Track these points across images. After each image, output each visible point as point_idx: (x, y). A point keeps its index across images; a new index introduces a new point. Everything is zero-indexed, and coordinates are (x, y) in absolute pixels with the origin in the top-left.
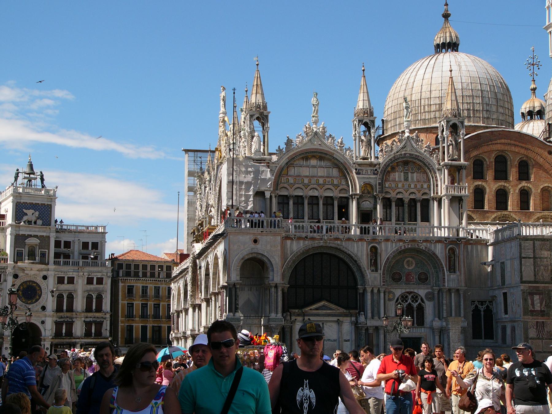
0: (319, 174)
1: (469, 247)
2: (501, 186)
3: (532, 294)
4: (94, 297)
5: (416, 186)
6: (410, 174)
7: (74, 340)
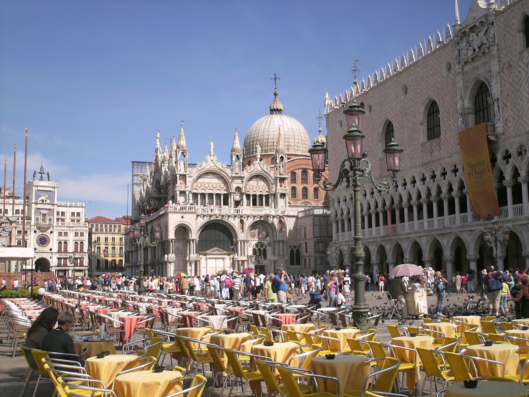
0: (213, 182)
3: (318, 243)
5: (262, 188)
7: (68, 268)
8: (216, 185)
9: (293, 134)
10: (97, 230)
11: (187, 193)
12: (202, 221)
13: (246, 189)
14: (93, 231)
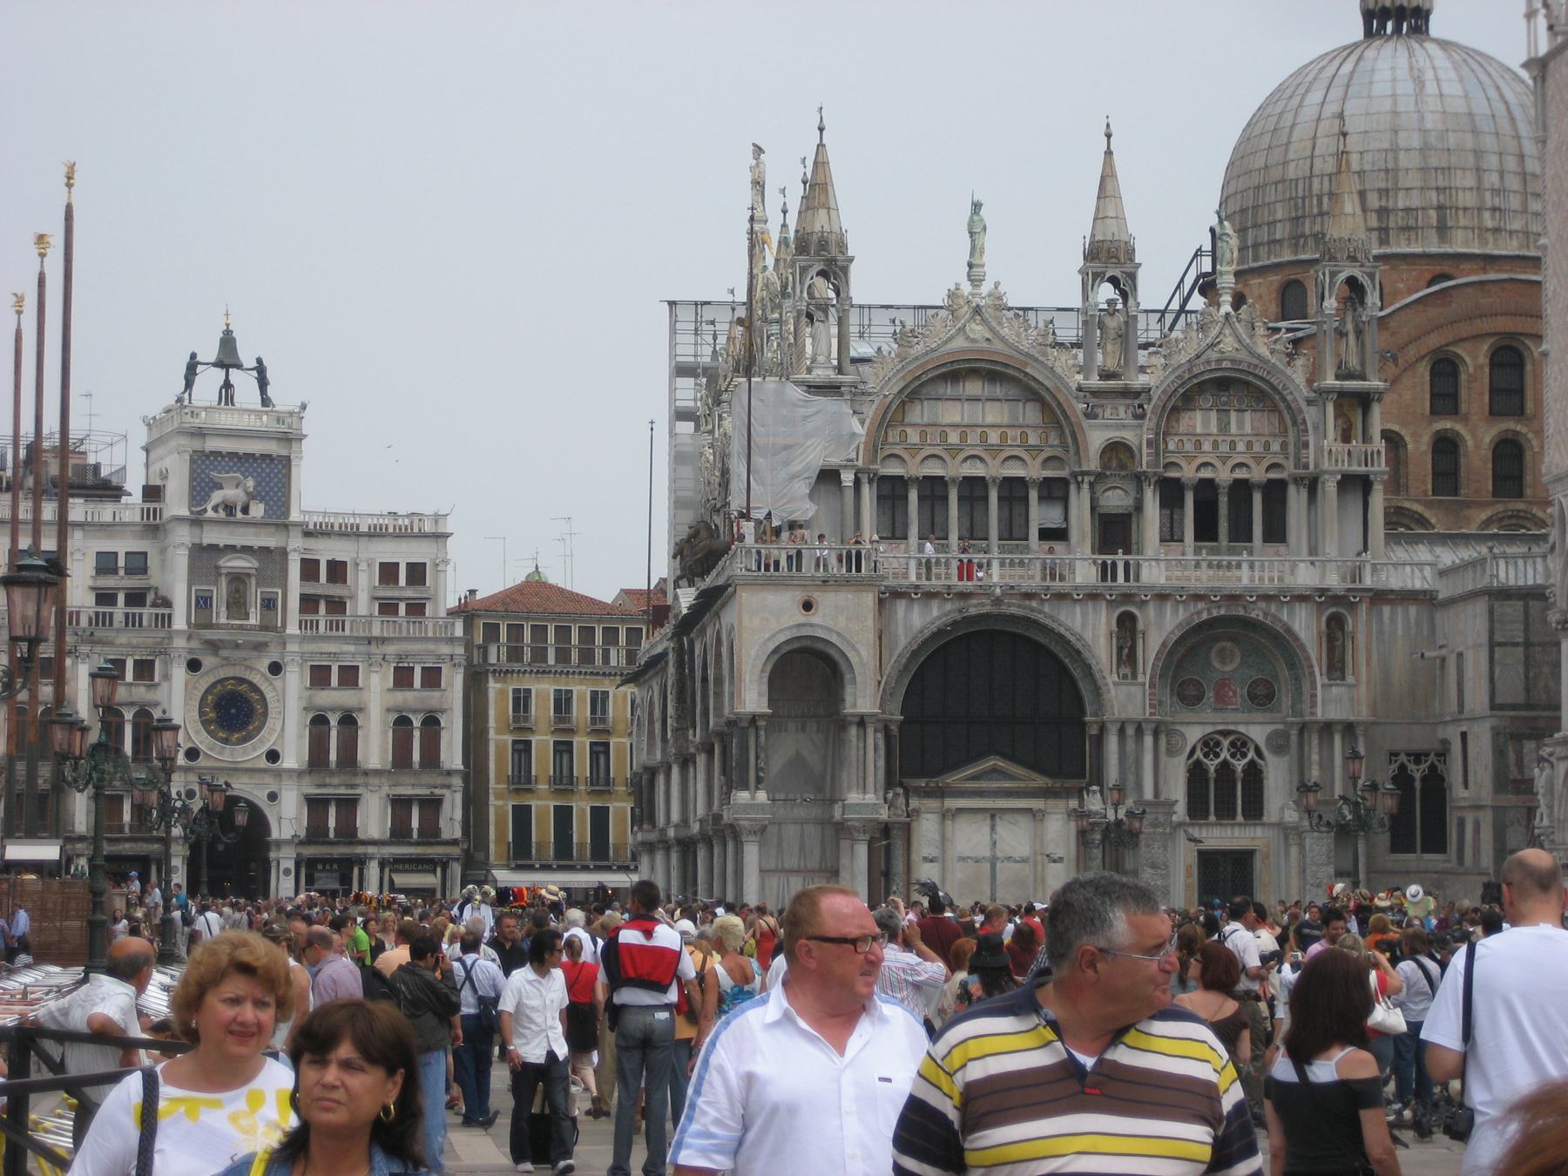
0: (989, 419)
1: (1386, 610)
2: (1506, 431)
3: (1517, 737)
4: (417, 723)
5: (1249, 445)
6: (1233, 415)
7: (360, 850)
8: (1003, 436)
9: (1469, 141)
10: (515, 654)
11: (847, 478)
12: (915, 621)
13: (1157, 454)
14: (493, 659)
